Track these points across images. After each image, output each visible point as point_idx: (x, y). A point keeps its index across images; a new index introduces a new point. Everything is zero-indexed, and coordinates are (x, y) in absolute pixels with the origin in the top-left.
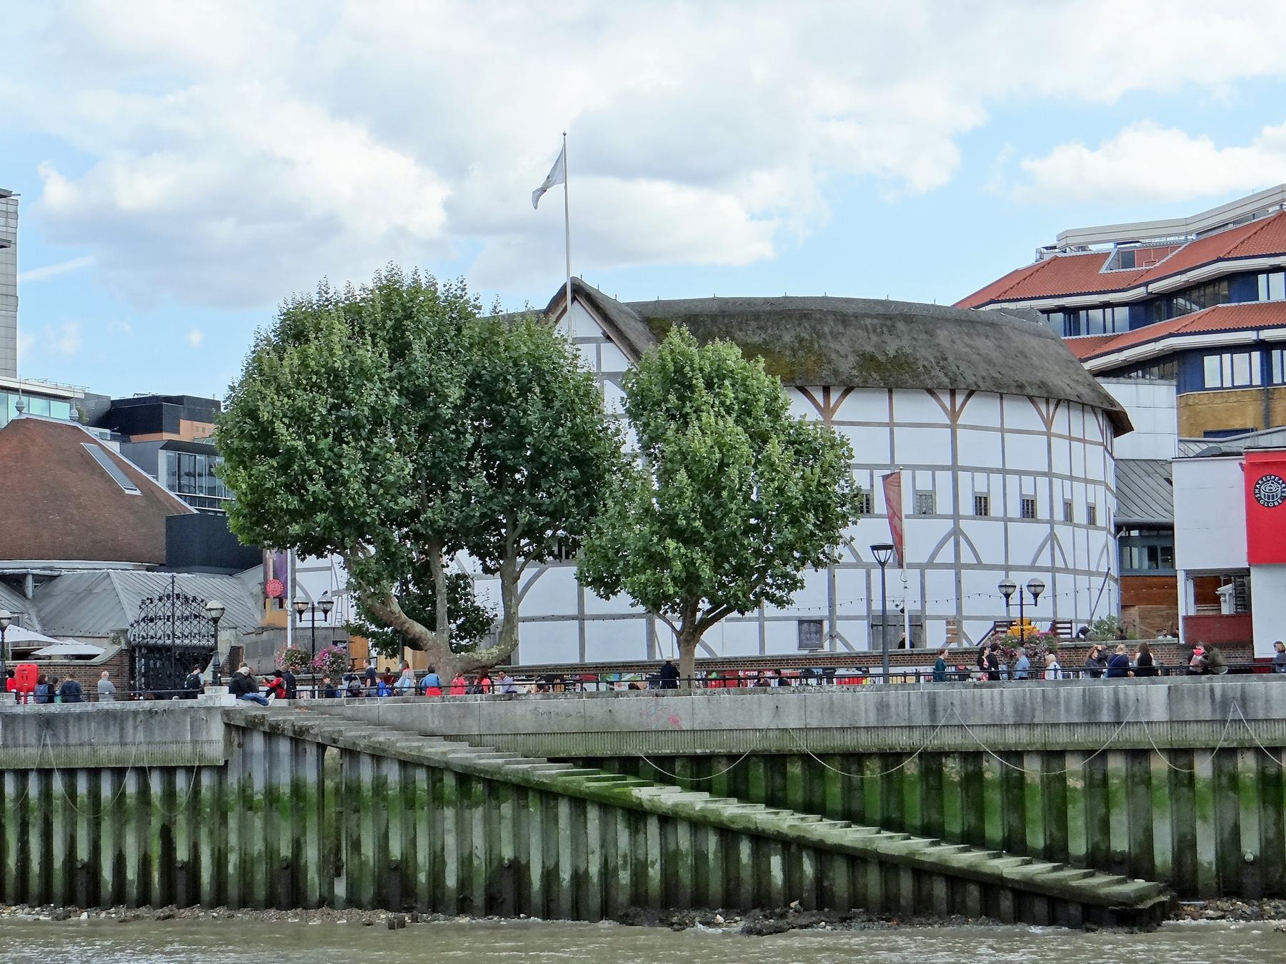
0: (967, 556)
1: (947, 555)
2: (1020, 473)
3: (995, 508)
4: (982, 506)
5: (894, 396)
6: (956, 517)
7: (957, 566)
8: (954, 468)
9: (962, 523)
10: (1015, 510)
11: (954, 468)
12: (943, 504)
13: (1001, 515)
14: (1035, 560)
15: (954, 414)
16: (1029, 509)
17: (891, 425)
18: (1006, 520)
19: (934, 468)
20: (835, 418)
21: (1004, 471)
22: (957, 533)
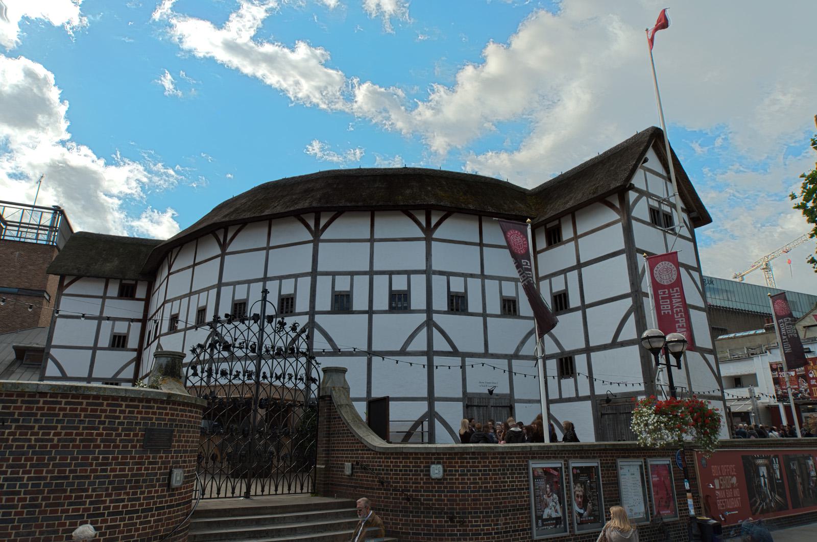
0: (440, 344)
1: (420, 343)
2: (500, 279)
3: (474, 304)
4: (457, 304)
5: (377, 221)
6: (429, 311)
7: (430, 353)
8: (429, 272)
9: (436, 317)
10: (494, 306)
11: (429, 272)
12: (418, 300)
13: (480, 311)
14: (518, 350)
15: (429, 230)
17: (372, 240)
18: (484, 315)
19: (408, 273)
20: (322, 237)
21: (483, 276)
22: (430, 324)
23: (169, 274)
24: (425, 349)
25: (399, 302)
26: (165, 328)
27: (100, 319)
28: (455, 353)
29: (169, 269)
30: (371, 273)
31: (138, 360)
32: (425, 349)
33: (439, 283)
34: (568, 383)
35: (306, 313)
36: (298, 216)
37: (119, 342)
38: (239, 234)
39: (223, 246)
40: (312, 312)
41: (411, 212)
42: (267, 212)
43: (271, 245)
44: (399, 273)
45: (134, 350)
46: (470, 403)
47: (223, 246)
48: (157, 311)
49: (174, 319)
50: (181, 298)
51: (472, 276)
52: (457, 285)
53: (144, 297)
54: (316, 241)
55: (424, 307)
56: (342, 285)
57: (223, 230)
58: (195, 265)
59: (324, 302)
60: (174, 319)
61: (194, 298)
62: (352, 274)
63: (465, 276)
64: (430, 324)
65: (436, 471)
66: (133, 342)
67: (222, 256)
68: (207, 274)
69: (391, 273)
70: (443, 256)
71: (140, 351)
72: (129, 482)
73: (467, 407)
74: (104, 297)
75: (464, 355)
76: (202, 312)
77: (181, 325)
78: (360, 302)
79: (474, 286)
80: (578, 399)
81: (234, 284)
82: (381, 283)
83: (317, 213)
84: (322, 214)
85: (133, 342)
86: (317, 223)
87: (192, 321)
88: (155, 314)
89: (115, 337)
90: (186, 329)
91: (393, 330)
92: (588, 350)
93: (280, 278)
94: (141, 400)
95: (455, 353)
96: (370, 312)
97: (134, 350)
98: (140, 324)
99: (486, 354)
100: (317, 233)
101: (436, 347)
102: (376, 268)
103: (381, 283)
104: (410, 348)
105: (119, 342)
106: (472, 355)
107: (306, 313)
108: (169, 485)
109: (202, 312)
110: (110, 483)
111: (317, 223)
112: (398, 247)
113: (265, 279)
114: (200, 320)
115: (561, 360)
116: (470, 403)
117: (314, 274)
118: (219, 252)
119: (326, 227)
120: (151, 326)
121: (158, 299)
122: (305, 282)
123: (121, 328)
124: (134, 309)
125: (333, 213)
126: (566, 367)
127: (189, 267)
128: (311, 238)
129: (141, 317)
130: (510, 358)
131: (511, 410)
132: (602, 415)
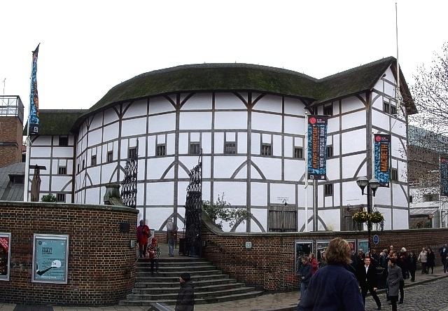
0: (255, 174)
1: (243, 174)
2: (294, 136)
4: (267, 150)
6: (249, 154)
7: (248, 180)
8: (249, 131)
9: (253, 159)
10: (289, 152)
12: (242, 148)
15: (250, 106)
16: (298, 153)
17: (213, 110)
18: (283, 158)
19: (236, 131)
20: (181, 109)
21: (283, 134)
22: (249, 162)
23: (88, 132)
24: (246, 178)
25: (230, 149)
26: (89, 163)
27: (51, 158)
28: (264, 180)
29: (88, 129)
30: (213, 131)
31: (73, 181)
32: (246, 178)
33: (255, 138)
34: (329, 199)
35: (173, 156)
36: (167, 97)
37: (62, 171)
38: (130, 107)
39: (120, 116)
40: (177, 155)
41: (239, 93)
42: (147, 95)
43: (150, 114)
44: (230, 131)
45: (70, 175)
46: (272, 210)
47: (120, 116)
48: (82, 153)
49: (94, 158)
50: (97, 146)
51: (276, 133)
52: (267, 139)
53: (73, 145)
54: (178, 112)
55: (245, 152)
56: (195, 138)
57: (119, 106)
58: (103, 126)
59: (184, 148)
60: (94, 158)
61: (105, 146)
62: (201, 131)
63: (272, 133)
64: (249, 162)
65: (248, 245)
66: (70, 171)
67: (120, 121)
68: (111, 132)
69: (225, 131)
70: (259, 121)
71: (73, 176)
72: (117, 244)
73: (270, 211)
74: (52, 146)
75: (269, 182)
76: (110, 154)
77: (98, 162)
78: (206, 148)
79: (277, 139)
80: (334, 208)
81: (129, 138)
82: (219, 138)
83: (178, 95)
84: (181, 95)
85: (70, 171)
86: (178, 101)
87: (105, 161)
88: (81, 155)
89: (60, 168)
90: (102, 164)
91: (225, 166)
92: (341, 181)
93: (157, 134)
94: (117, 211)
95: (264, 180)
96: (212, 155)
97: (70, 175)
98: (72, 160)
99: (283, 181)
100: (178, 107)
101: (252, 177)
102: (215, 128)
103: (219, 138)
104: (236, 178)
105: (62, 171)
106: (274, 182)
107: (173, 156)
108: (130, 246)
109: (110, 154)
110: (111, 244)
111: (178, 101)
112: (231, 116)
113: (147, 134)
114: (110, 160)
115: (326, 185)
116: (272, 210)
117: (177, 132)
118: (118, 119)
119: (183, 103)
120: (77, 160)
121: (82, 146)
122: (172, 137)
123: (63, 163)
124: (66, 152)
125: (188, 94)
126: (329, 191)
127: (100, 128)
128: (175, 110)
129: (72, 156)
130: (297, 183)
131: (296, 212)
132: (345, 217)
